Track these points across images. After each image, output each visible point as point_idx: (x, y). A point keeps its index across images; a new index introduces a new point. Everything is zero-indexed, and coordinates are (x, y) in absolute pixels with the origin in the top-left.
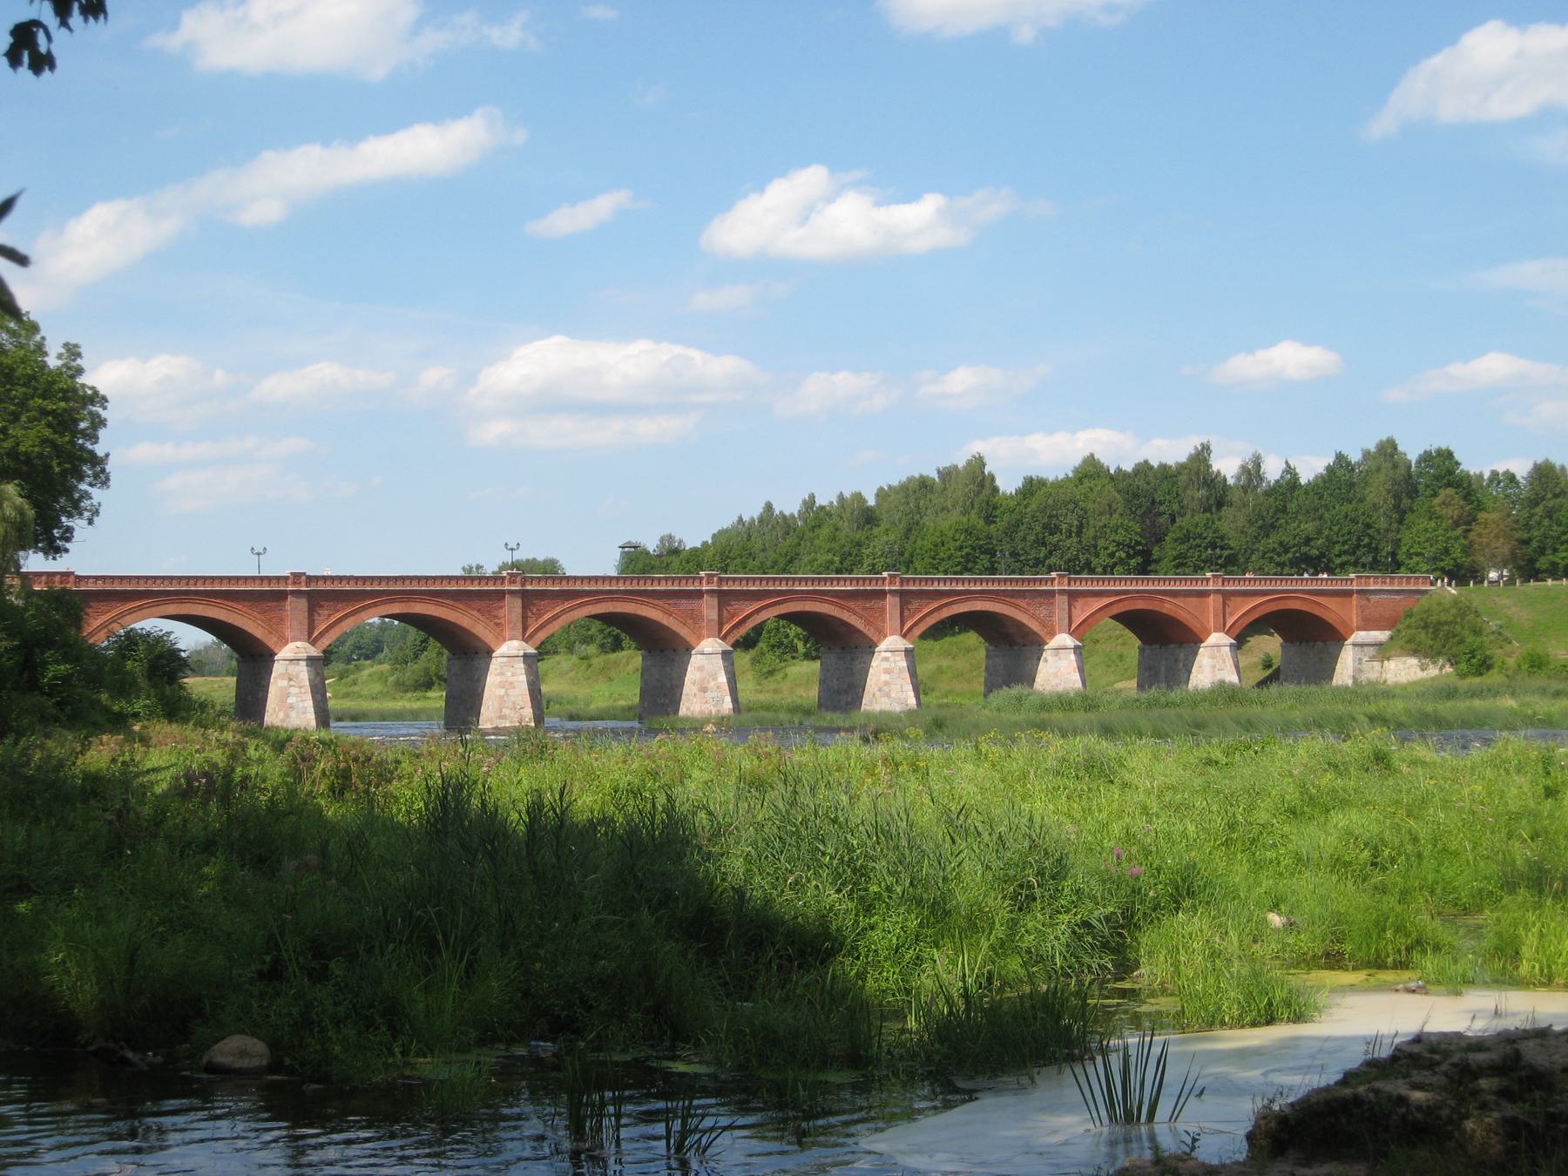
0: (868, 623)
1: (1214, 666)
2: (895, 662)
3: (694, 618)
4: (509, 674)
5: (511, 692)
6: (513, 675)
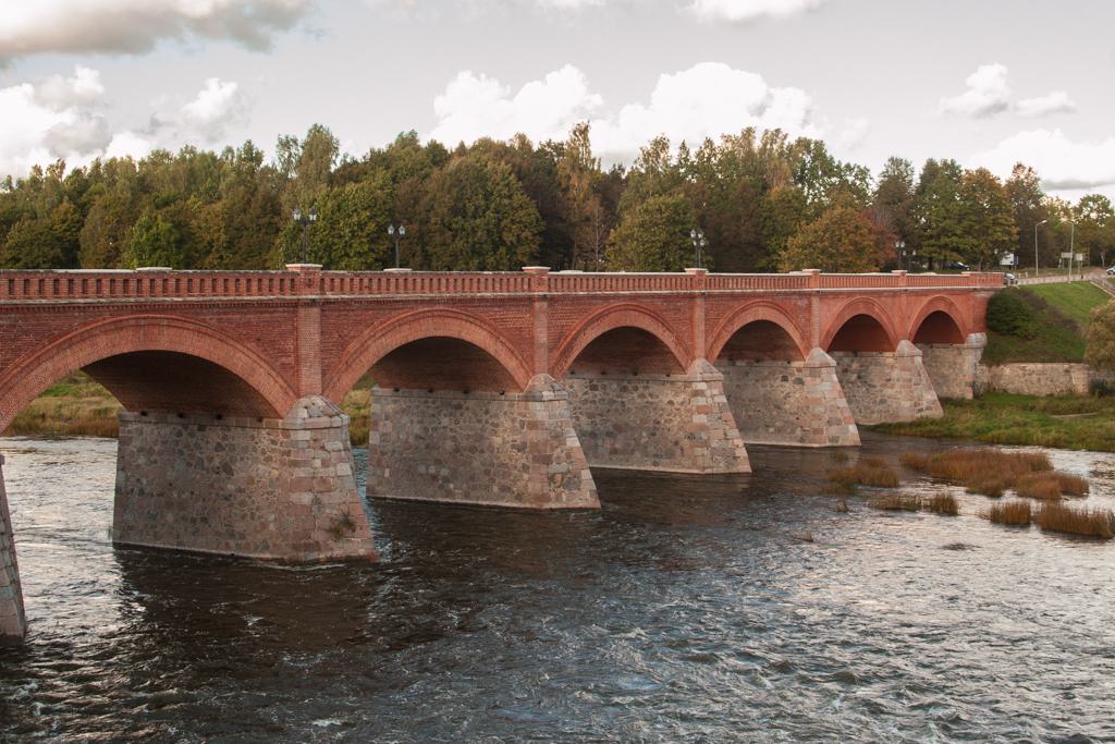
0: (679, 341)
1: (910, 380)
2: (713, 396)
3: (522, 342)
4: (318, 463)
5: (325, 499)
6: (325, 464)
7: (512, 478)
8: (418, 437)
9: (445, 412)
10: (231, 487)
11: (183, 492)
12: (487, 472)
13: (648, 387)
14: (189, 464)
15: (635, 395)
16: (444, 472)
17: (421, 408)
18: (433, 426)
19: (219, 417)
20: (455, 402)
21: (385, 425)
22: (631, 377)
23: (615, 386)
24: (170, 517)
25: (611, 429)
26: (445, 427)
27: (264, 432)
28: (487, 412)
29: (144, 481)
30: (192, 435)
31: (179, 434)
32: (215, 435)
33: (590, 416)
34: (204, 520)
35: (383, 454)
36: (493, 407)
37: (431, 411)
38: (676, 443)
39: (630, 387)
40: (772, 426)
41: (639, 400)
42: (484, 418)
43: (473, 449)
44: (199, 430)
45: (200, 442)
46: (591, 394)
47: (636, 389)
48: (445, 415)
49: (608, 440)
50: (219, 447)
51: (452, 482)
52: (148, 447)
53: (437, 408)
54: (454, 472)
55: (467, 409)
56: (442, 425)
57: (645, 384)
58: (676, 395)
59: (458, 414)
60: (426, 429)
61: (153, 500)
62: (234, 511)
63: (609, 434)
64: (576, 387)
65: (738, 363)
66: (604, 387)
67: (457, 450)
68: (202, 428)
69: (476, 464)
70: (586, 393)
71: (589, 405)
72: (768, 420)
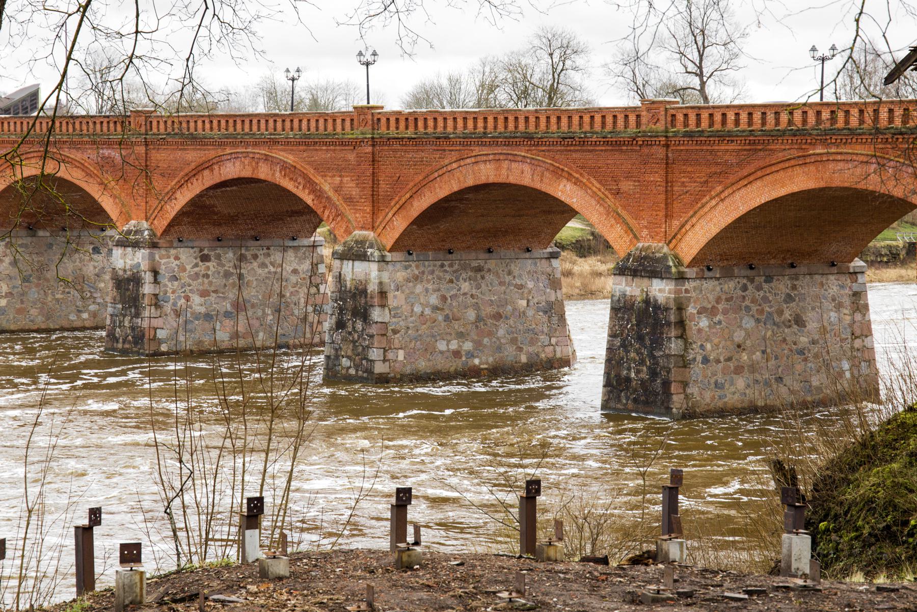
7: (540, 344)
8: (436, 308)
9: (464, 275)
10: (804, 340)
11: (754, 353)
12: (514, 341)
13: (269, 255)
14: (758, 321)
15: (255, 264)
16: (468, 346)
17: (437, 273)
18: (452, 293)
19: (792, 266)
20: (474, 264)
21: (395, 297)
22: (252, 243)
23: (230, 255)
24: (741, 383)
25: (229, 307)
26: (465, 294)
27: (832, 277)
28: (510, 273)
29: (708, 346)
30: (759, 288)
31: (744, 288)
32: (782, 286)
33: (204, 294)
34: (780, 379)
35: (395, 332)
36: (515, 268)
37: (448, 277)
38: (305, 319)
39: (249, 255)
40: (85, 312)
41: (260, 271)
42: (508, 279)
43: (498, 316)
44: (766, 281)
45: (768, 294)
46: (202, 266)
47: (255, 257)
48: (465, 280)
49: (228, 323)
50: (789, 298)
51: (477, 357)
52: (710, 306)
53: (455, 272)
54: (478, 344)
55: (489, 270)
56: (462, 292)
57: (265, 251)
58: (300, 263)
59: (479, 276)
60: (444, 298)
61: (720, 366)
62: (809, 365)
63: (227, 314)
64: (183, 257)
65: (41, 233)
66: (218, 257)
67: (479, 319)
68: (769, 279)
69: (501, 332)
70: (196, 265)
71: (200, 280)
72: (79, 303)
